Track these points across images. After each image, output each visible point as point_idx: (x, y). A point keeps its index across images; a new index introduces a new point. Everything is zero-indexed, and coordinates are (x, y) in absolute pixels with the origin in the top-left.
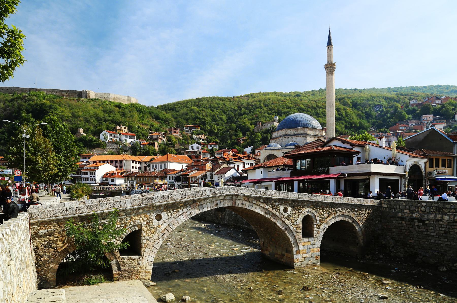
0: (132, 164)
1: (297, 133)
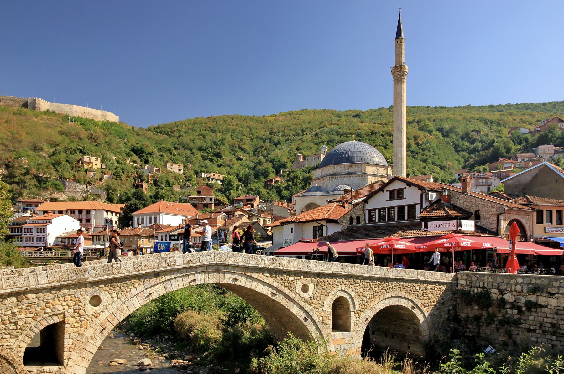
1: (350, 171)
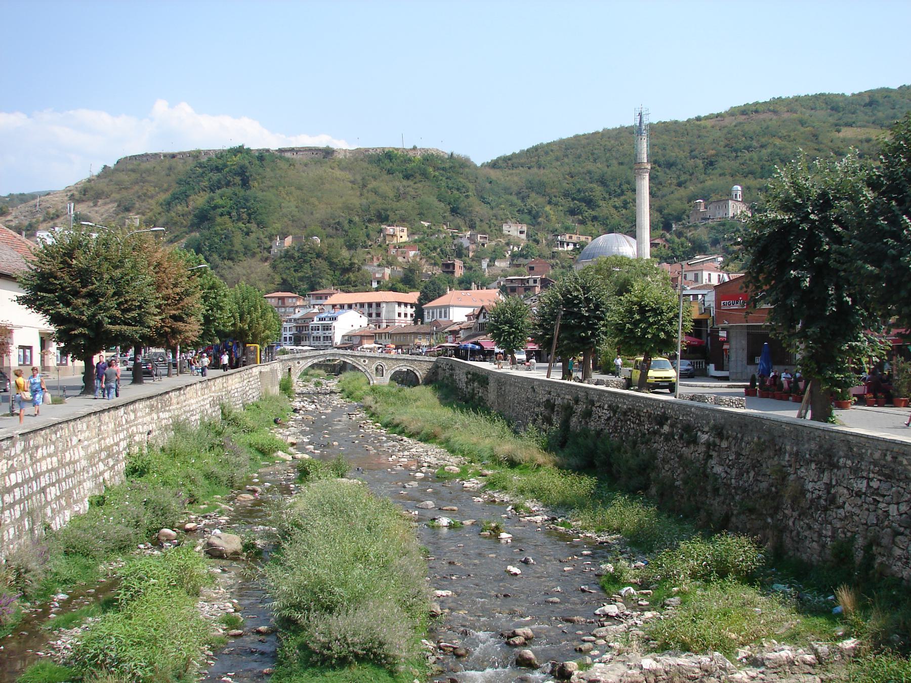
0: (397, 309)
